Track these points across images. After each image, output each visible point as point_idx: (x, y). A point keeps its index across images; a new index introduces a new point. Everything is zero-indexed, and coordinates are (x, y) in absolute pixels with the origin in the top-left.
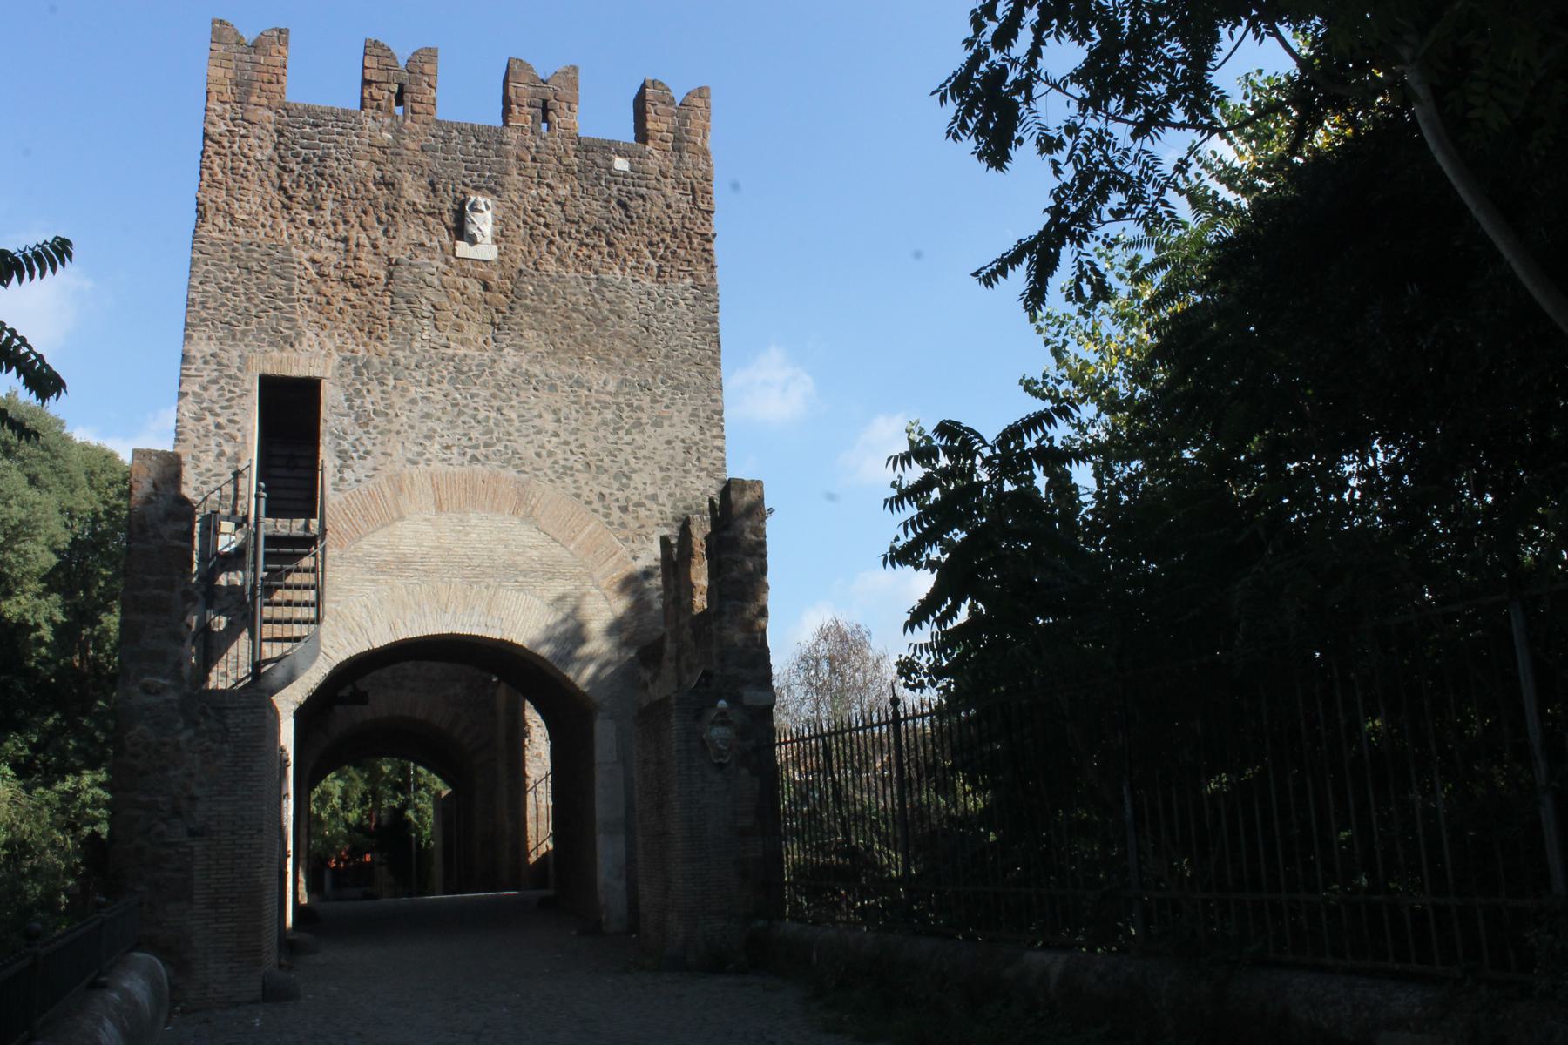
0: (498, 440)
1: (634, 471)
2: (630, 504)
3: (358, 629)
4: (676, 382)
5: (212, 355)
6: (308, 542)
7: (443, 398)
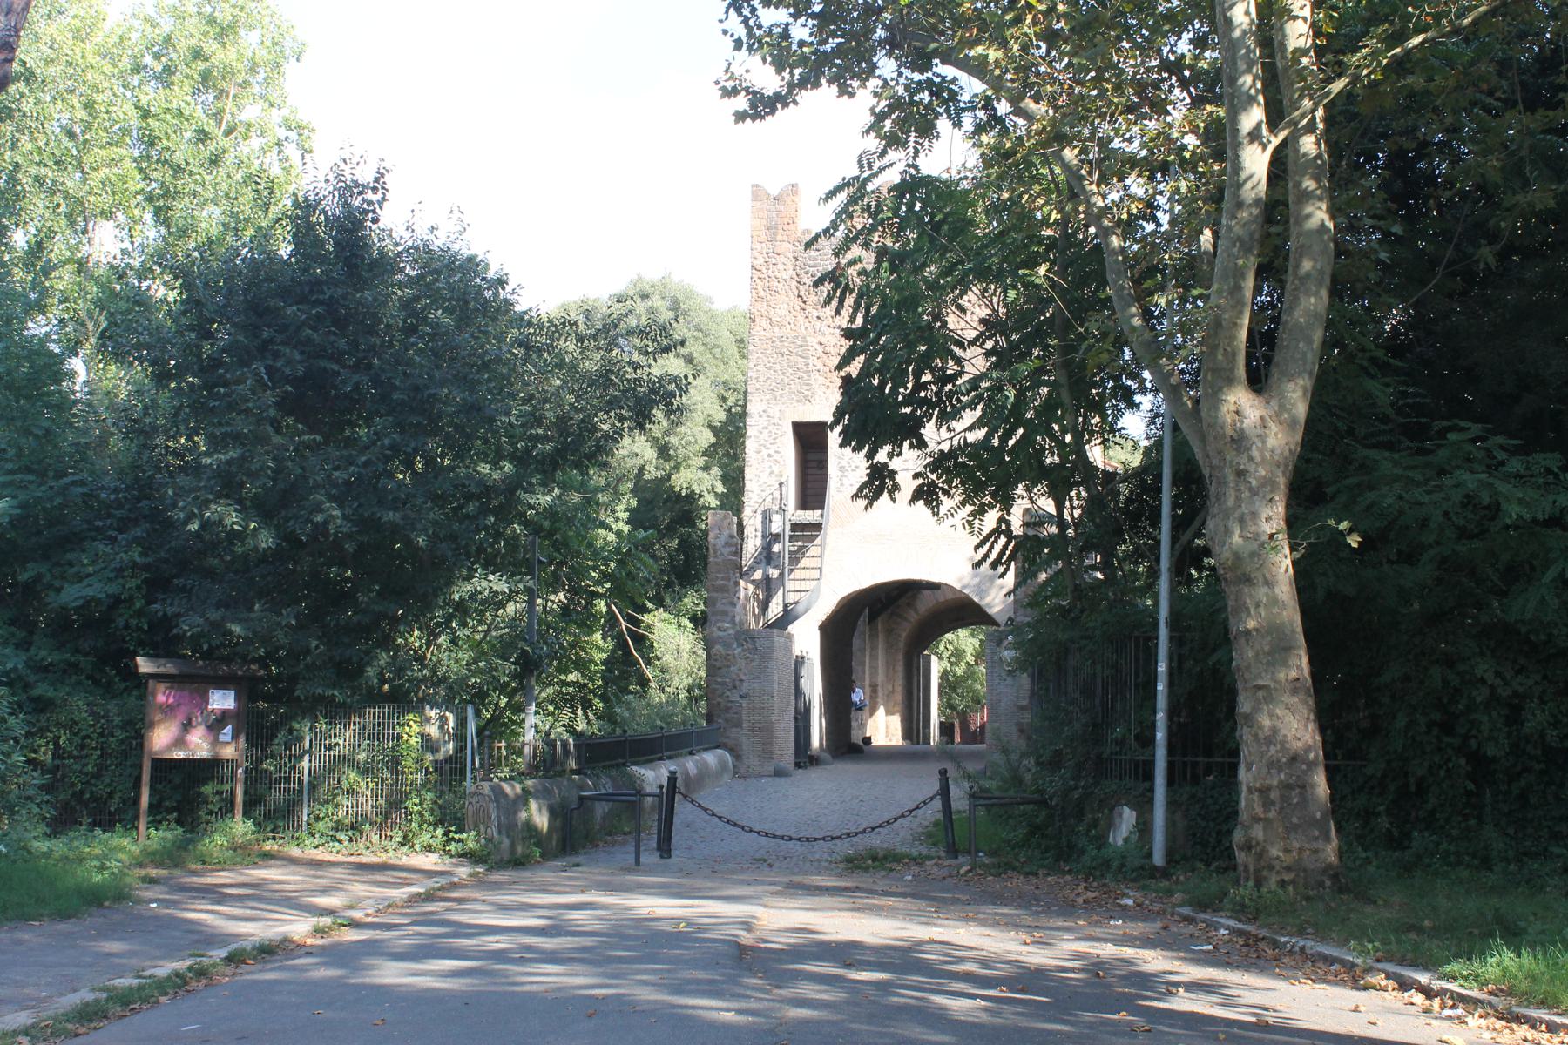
6: (817, 527)
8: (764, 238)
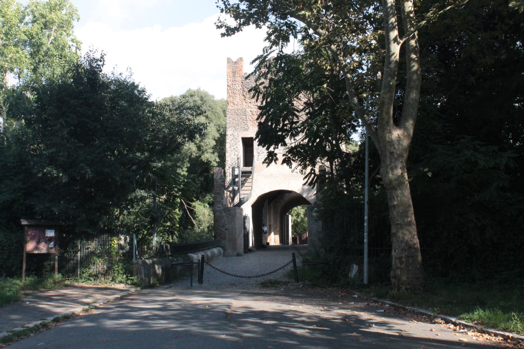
6: (250, 172)
8: (231, 76)
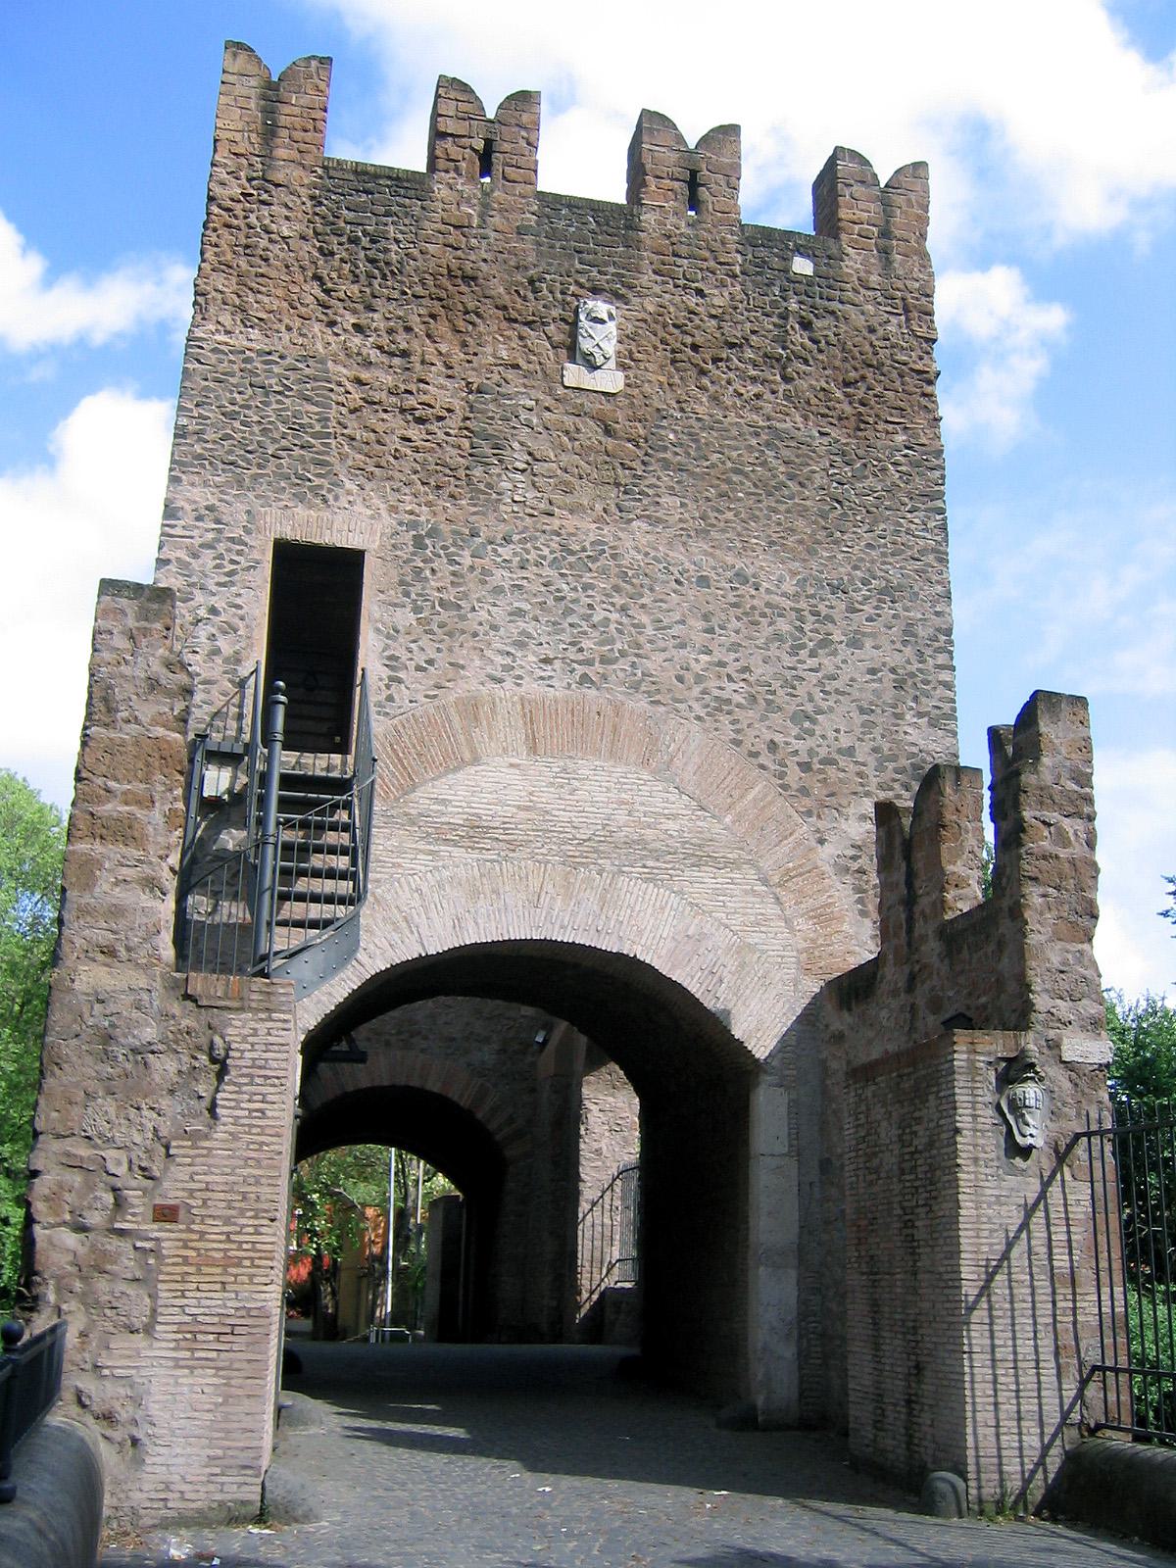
0: (623, 654)
1: (820, 712)
2: (815, 760)
3: (404, 925)
4: (884, 584)
5: (207, 508)
6: (342, 786)
7: (543, 589)
